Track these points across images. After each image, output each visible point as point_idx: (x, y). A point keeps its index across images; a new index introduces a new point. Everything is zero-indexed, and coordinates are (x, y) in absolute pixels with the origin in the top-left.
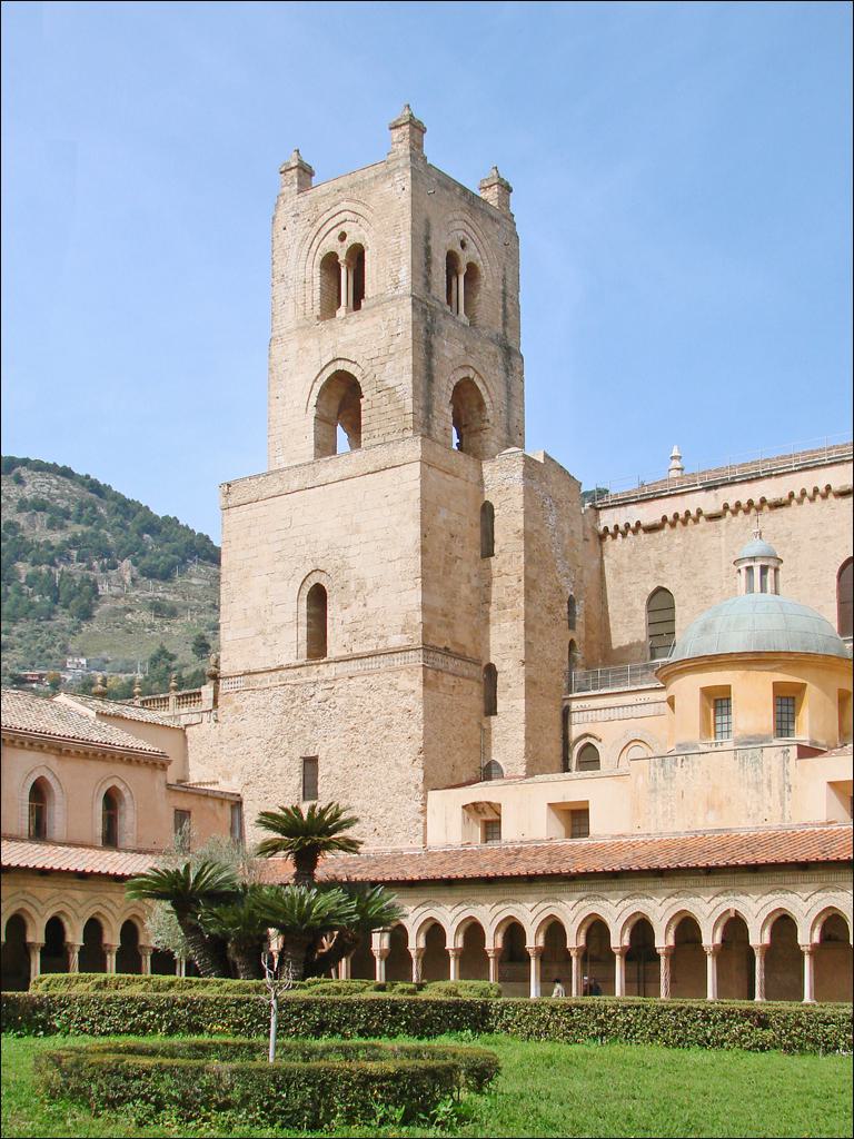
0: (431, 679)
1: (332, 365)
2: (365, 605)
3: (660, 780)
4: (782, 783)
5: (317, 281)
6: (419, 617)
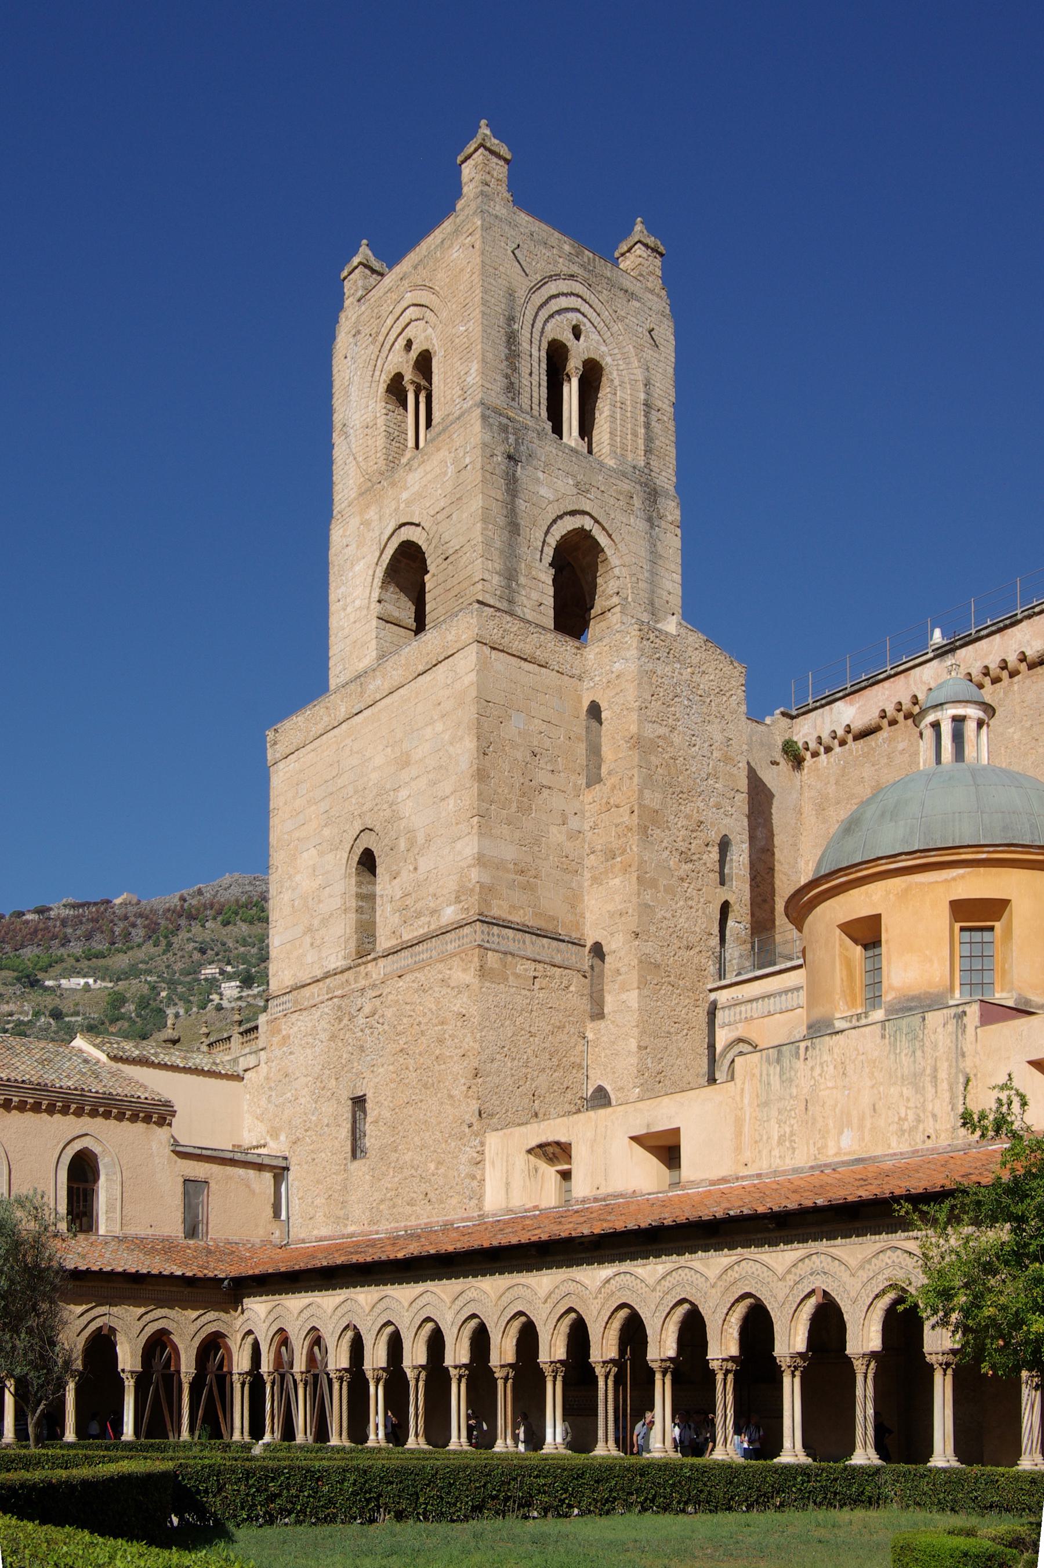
0: (496, 966)
1: (394, 538)
3: (775, 1081)
4: (953, 1071)
5: (381, 421)
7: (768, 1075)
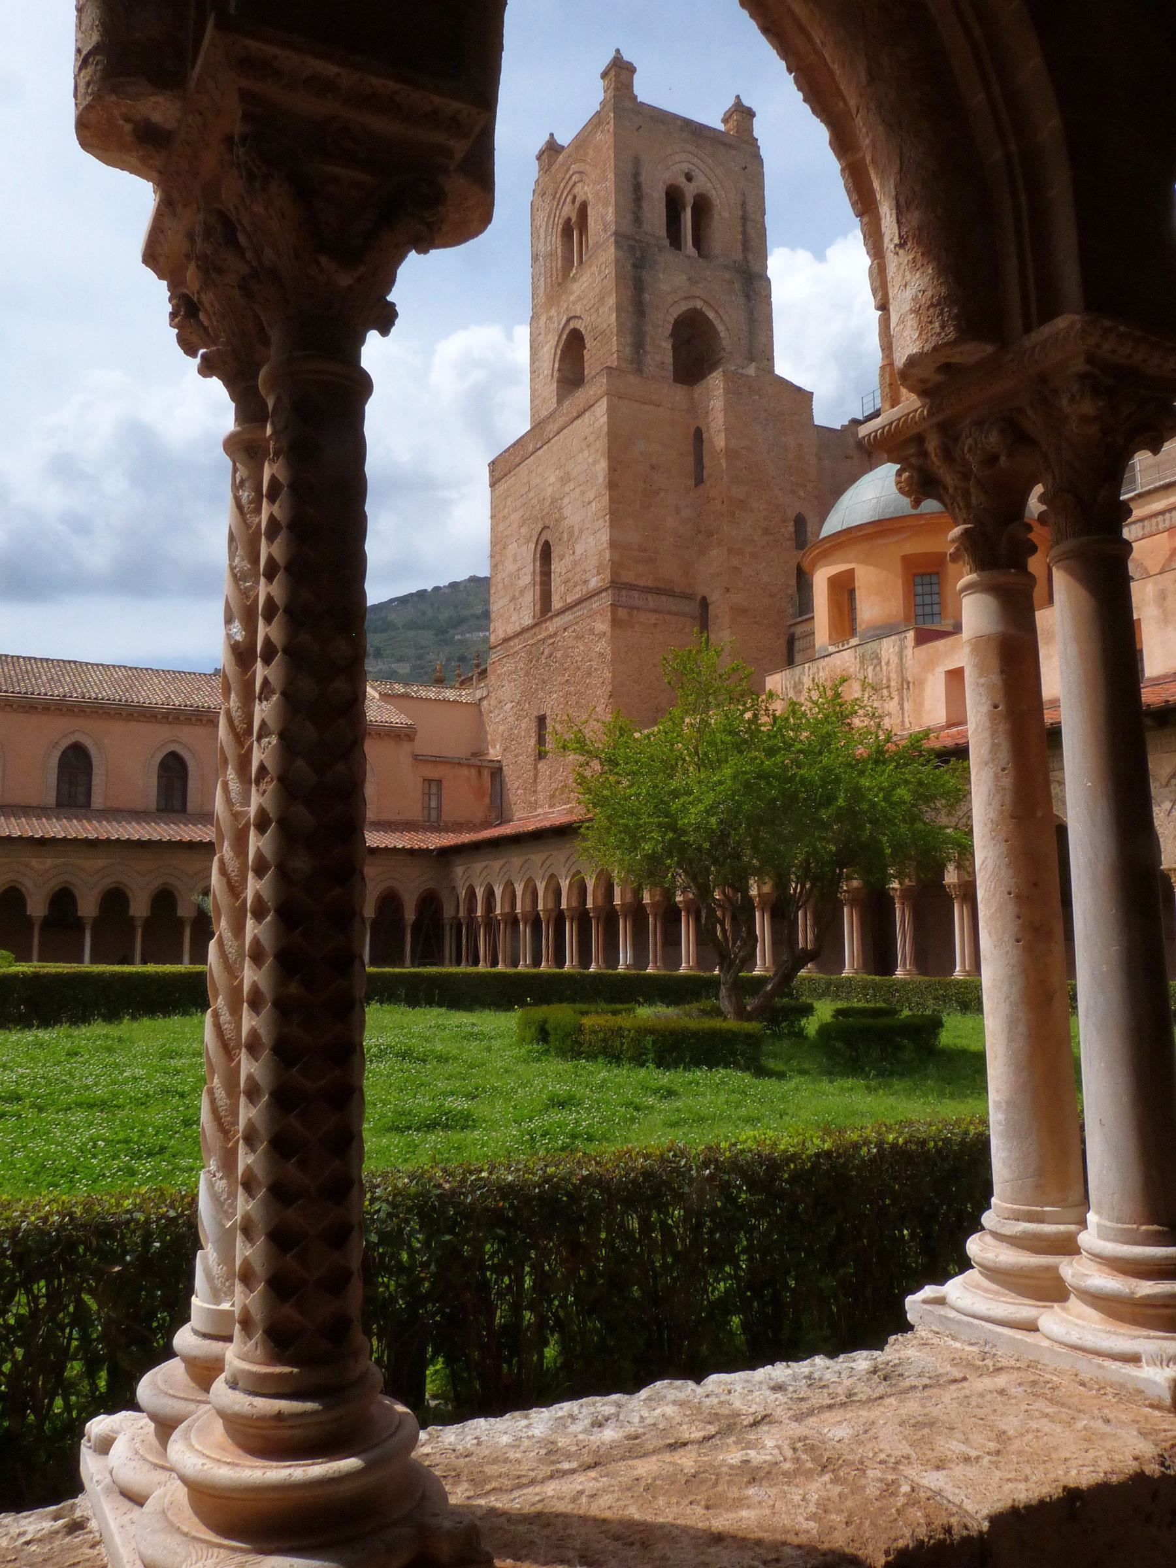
2: (574, 553)
6: (607, 556)
7: (786, 688)
